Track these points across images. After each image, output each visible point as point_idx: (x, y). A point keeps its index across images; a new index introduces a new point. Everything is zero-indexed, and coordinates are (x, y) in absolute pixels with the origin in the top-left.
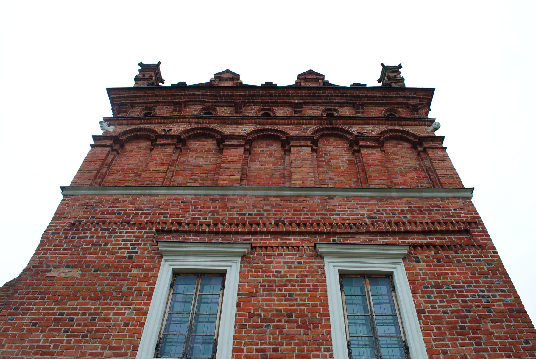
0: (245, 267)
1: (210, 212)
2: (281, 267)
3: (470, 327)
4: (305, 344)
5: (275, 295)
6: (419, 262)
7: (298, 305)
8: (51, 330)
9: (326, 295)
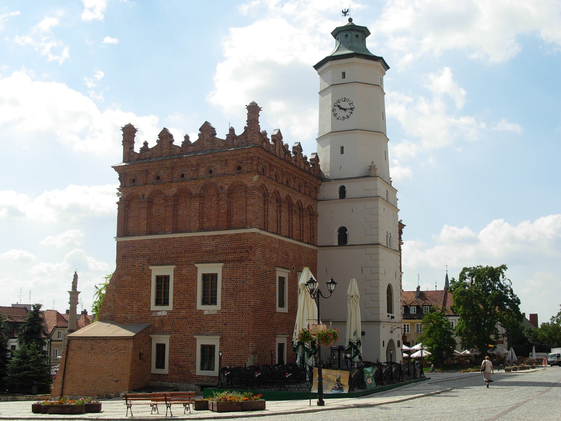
0: (175, 273)
1: (164, 247)
3: (235, 294)
4: (190, 300)
6: (227, 268)
7: (190, 287)
8: (129, 298)
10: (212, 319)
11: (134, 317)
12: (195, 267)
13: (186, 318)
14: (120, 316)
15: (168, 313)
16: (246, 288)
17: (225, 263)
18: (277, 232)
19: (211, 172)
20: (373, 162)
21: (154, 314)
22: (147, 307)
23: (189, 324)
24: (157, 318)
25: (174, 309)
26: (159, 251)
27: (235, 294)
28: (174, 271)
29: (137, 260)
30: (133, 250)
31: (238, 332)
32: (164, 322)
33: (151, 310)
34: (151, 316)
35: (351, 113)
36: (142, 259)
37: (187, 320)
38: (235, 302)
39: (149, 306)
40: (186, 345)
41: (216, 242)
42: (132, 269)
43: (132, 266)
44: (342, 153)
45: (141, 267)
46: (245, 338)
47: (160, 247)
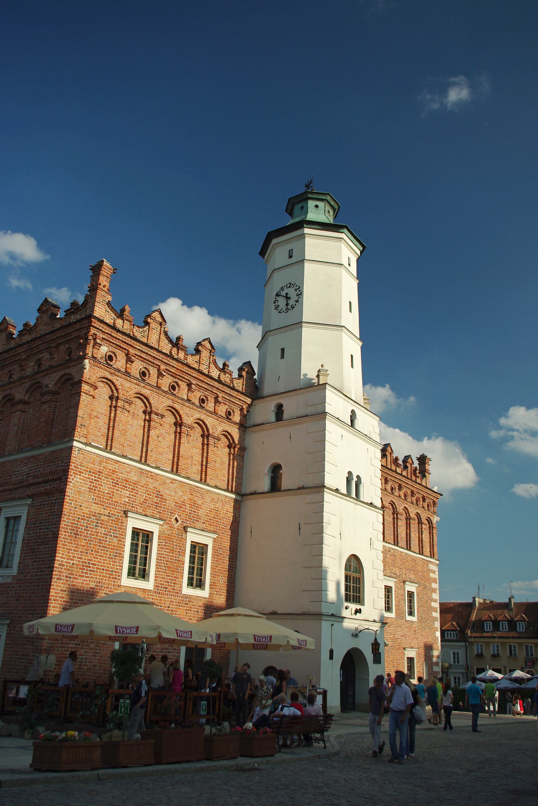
17: (33, 499)
18: (228, 488)
19: (40, 365)
20: (322, 366)
27: (36, 549)
35: (297, 301)
41: (29, 468)
44: (282, 357)
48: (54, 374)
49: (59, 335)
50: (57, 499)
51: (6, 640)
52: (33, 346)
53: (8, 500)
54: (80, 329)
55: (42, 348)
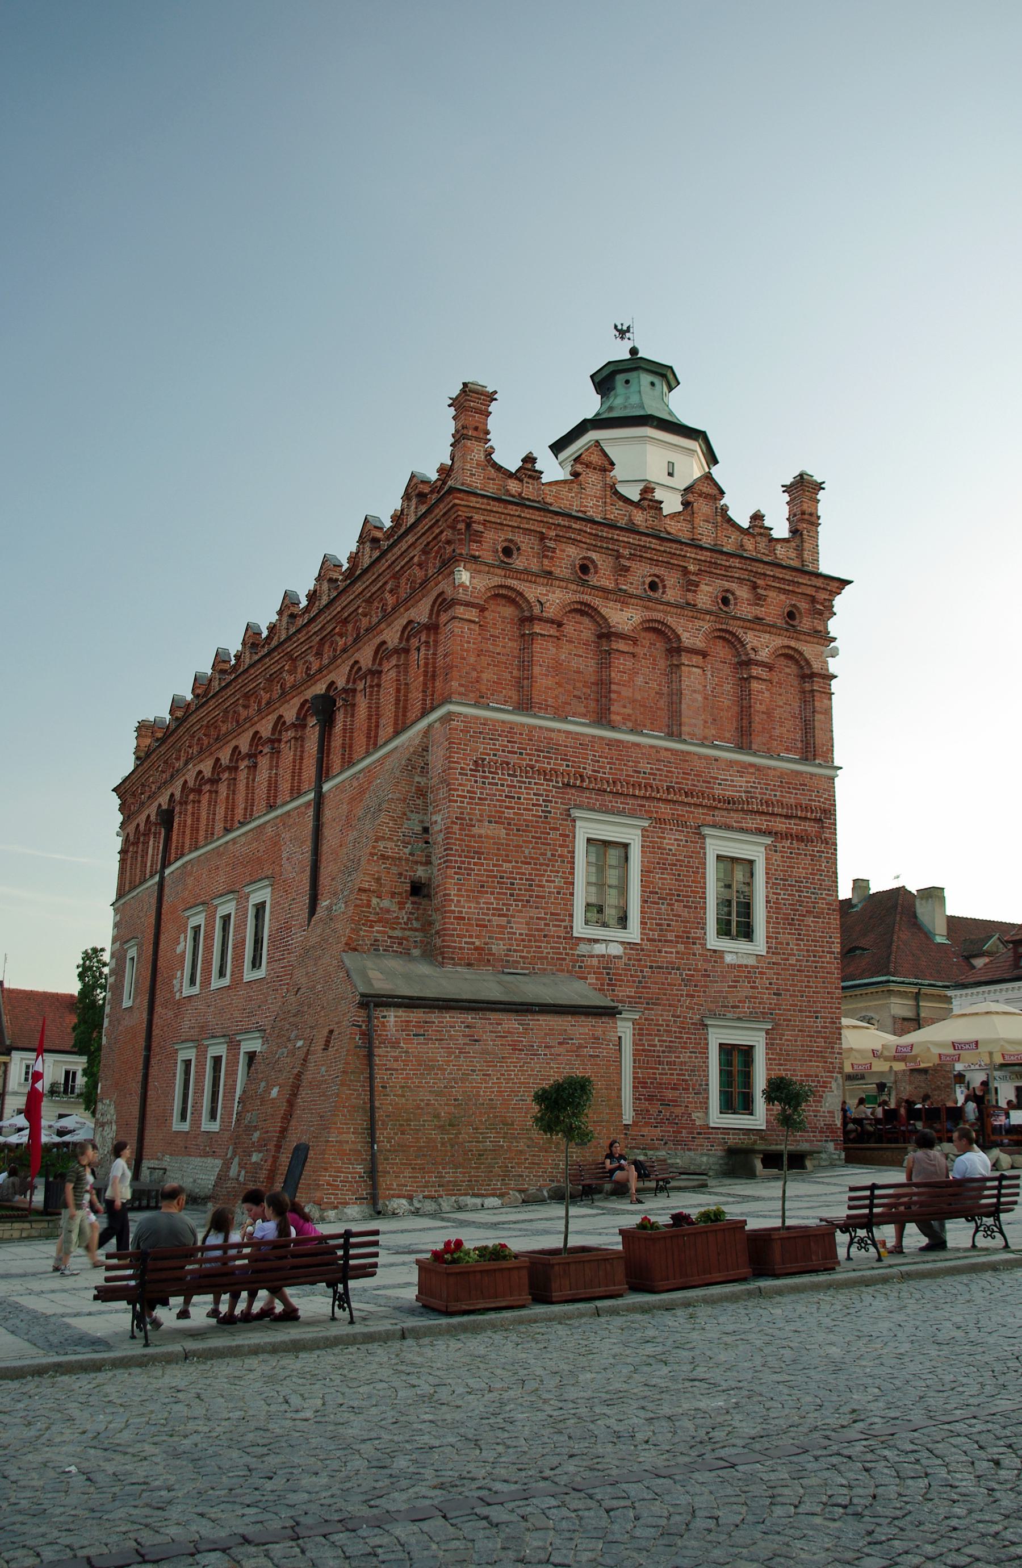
1: (608, 763)
2: (673, 845)
3: (798, 920)
4: (688, 922)
5: (668, 874)
6: (776, 851)
7: (684, 886)
8: (498, 893)
9: (705, 878)
10: (746, 977)
11: (515, 951)
12: (700, 834)
13: (678, 969)
14: (466, 943)
15: (625, 948)
16: (823, 909)
19: (725, 601)
21: (583, 949)
22: (560, 926)
23: (686, 986)
24: (595, 961)
25: (642, 939)
26: (594, 771)
27: (798, 920)
28: (643, 836)
29: (525, 783)
30: (509, 752)
31: (807, 1017)
32: (614, 974)
33: (575, 935)
34: (573, 955)
36: (542, 785)
37: (681, 975)
38: (797, 939)
39: (566, 923)
40: (680, 1043)
41: (747, 782)
42: (507, 808)
43: (506, 796)
45: (541, 806)
46: (825, 1032)
47: (598, 761)
48: (767, 636)
49: (781, 576)
50: (823, 852)
51: (767, 1054)
52: (724, 563)
53: (714, 826)
54: (819, 588)
55: (737, 575)
